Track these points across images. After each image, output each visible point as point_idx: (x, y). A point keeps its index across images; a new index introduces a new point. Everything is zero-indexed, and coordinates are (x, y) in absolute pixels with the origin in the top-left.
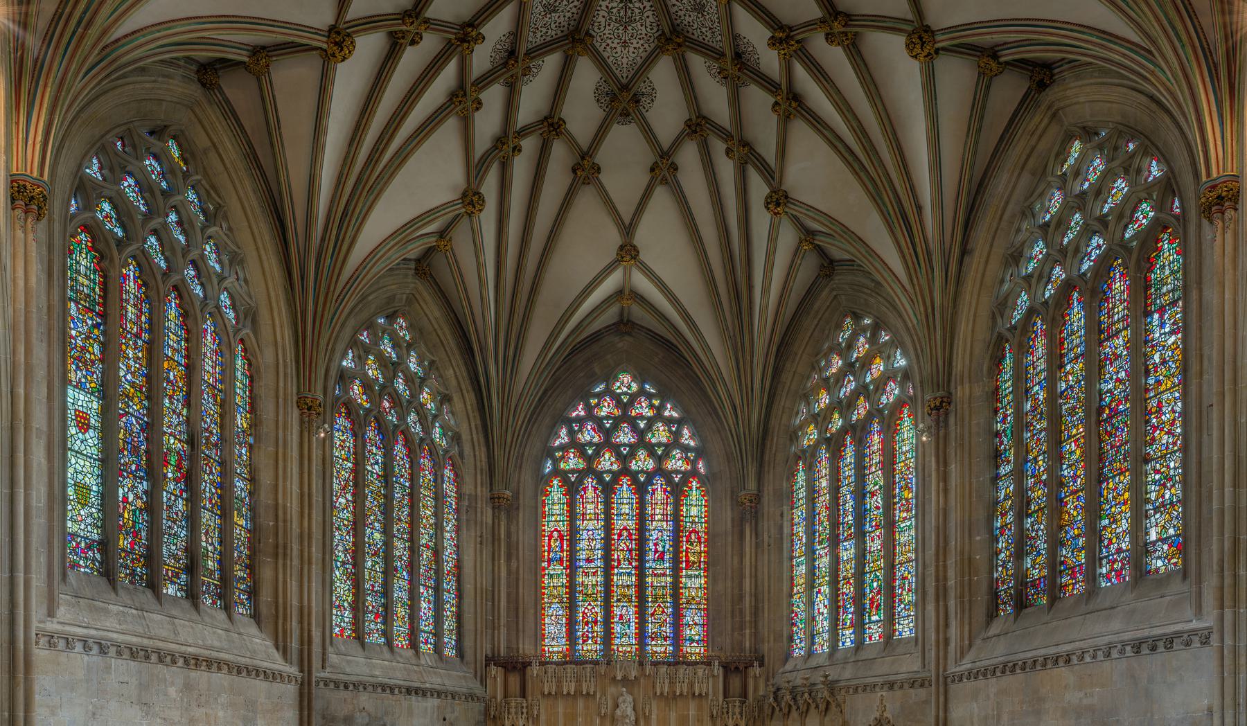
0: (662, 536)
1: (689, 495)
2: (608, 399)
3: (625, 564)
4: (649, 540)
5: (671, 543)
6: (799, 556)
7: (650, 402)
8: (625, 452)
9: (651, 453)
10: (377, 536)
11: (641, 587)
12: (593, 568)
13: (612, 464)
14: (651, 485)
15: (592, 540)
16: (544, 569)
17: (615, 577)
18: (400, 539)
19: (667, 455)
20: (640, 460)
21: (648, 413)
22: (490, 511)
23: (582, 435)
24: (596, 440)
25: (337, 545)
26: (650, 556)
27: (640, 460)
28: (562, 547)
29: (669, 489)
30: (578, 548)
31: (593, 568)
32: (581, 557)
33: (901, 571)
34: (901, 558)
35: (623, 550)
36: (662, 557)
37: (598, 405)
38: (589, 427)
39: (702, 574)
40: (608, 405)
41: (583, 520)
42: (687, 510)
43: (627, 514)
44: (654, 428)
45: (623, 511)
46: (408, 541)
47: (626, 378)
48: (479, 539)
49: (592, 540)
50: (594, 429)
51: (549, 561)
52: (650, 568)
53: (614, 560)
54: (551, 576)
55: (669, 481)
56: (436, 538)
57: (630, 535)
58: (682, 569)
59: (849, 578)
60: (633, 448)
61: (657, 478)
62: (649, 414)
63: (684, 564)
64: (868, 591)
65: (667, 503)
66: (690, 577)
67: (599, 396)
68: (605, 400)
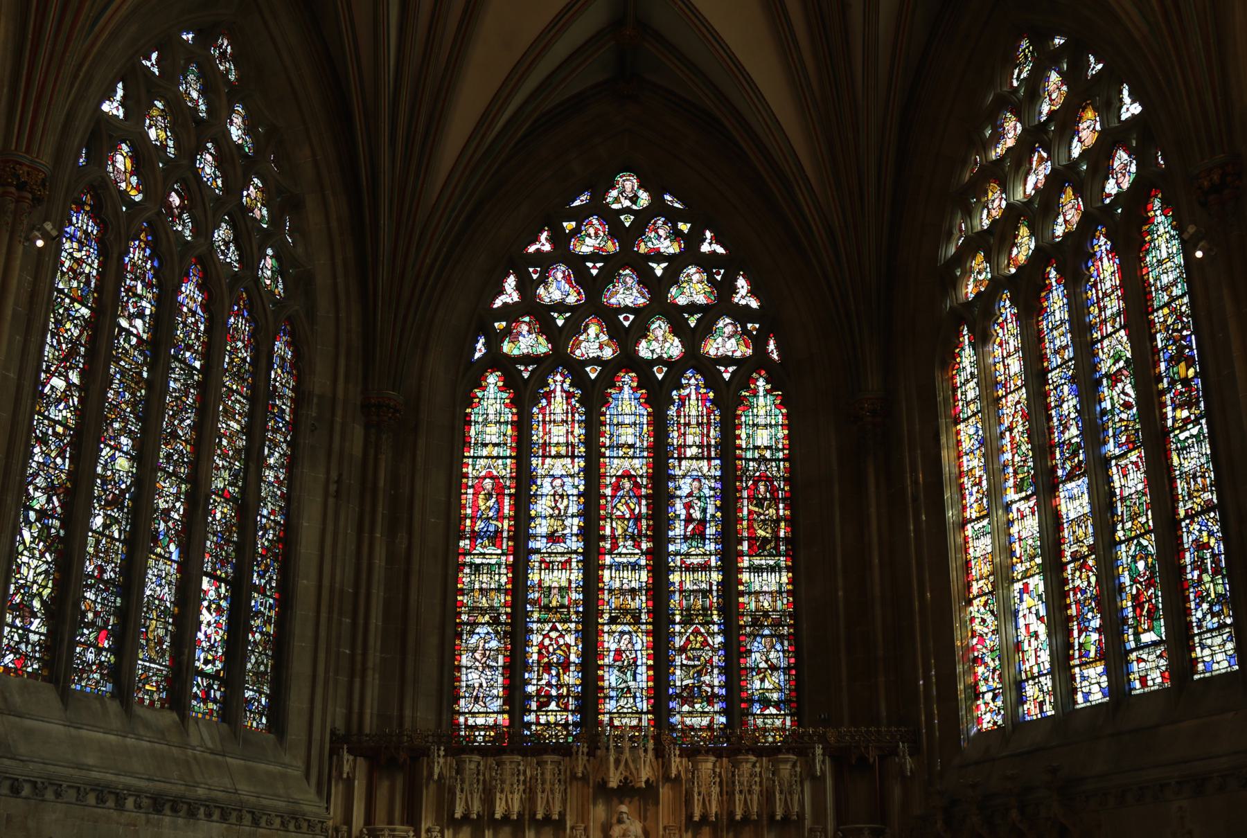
0: (700, 489)
1: (751, 407)
2: (595, 222)
3: (626, 547)
4: (674, 497)
5: (718, 503)
6: (977, 519)
7: (675, 227)
8: (626, 324)
9: (678, 328)
10: (122, 463)
11: (659, 590)
12: (562, 554)
13: (601, 348)
15: (562, 496)
17: (606, 573)
18: (170, 475)
19: (706, 329)
20: (656, 339)
21: (669, 247)
22: (358, 431)
24: (572, 299)
25: (35, 475)
26: (678, 529)
27: (656, 339)
28: (499, 510)
29: (711, 395)
30: (533, 513)
31: (562, 554)
32: (539, 530)
33: (1191, 533)
34: (1189, 505)
35: (622, 518)
36: (699, 535)
37: (576, 232)
38: (559, 275)
39: (783, 564)
40: (596, 235)
41: (544, 457)
42: (748, 436)
43: (632, 446)
44: (682, 277)
45: (622, 440)
46: (183, 481)
47: (629, 183)
48: (333, 488)
49: (562, 496)
50: (567, 279)
51: (474, 536)
52: (677, 553)
53: (604, 538)
54: (477, 568)
55: (712, 380)
56: (245, 480)
57: (637, 486)
58: (741, 554)
59: (1085, 557)
60: (643, 317)
61: (689, 374)
62: (671, 251)
63: (746, 544)
64: (1126, 580)
65: (709, 424)
66: (757, 570)
67: (581, 216)
68: (592, 225)
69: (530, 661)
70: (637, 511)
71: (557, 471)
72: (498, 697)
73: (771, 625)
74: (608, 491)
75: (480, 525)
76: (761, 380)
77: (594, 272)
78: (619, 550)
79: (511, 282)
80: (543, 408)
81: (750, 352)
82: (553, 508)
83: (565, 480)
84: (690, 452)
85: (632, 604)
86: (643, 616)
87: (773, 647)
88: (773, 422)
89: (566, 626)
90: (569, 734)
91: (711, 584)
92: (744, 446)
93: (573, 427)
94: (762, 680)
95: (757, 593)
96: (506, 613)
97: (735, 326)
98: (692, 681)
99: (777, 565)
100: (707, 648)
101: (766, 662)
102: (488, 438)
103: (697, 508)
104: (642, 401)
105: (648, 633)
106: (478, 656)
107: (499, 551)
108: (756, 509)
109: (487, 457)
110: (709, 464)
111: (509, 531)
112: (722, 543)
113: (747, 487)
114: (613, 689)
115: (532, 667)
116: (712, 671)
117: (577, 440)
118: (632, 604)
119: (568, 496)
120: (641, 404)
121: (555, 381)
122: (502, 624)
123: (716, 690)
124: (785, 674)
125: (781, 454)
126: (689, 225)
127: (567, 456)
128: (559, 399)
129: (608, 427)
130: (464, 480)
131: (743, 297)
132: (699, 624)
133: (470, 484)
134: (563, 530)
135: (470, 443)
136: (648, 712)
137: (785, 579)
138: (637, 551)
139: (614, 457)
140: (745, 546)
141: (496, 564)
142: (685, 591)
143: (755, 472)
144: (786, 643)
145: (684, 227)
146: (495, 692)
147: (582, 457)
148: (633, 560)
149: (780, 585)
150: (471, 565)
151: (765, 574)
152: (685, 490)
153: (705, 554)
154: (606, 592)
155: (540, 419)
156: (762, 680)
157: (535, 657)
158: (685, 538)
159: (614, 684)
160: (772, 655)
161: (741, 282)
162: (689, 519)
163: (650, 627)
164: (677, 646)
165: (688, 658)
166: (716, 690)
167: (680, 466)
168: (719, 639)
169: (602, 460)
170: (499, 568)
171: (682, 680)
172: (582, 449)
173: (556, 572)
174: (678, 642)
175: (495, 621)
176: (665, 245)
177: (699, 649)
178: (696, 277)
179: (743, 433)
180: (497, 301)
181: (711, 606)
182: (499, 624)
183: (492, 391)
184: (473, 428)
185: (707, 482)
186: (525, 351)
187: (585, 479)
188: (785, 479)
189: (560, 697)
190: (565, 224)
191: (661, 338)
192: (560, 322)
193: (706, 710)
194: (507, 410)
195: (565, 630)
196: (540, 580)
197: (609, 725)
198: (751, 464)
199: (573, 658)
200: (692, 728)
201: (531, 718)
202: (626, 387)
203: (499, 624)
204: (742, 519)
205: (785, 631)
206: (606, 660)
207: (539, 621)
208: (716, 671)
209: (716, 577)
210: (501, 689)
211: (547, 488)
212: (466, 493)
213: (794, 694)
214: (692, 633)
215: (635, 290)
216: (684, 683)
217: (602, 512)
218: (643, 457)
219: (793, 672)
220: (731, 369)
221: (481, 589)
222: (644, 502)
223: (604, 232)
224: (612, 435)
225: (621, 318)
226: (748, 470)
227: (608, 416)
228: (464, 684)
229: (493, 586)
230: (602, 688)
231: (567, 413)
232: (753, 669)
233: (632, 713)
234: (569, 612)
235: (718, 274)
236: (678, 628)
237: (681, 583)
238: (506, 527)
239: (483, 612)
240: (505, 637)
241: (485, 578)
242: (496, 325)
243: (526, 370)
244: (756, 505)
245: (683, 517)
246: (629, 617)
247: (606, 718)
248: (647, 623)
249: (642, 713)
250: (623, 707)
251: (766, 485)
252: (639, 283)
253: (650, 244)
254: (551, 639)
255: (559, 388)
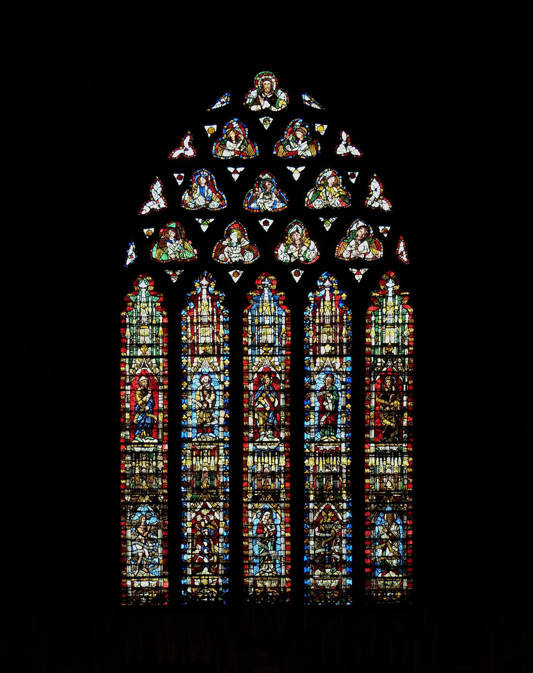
0: (332, 383)
2: (235, 125)
5: (348, 396)
7: (312, 128)
8: (266, 228)
12: (211, 443)
14: (314, 292)
15: (209, 392)
16: (128, 443)
20: (294, 244)
23: (191, 195)
24: (215, 205)
26: (313, 420)
27: (294, 244)
28: (154, 404)
29: (344, 296)
30: (184, 406)
31: (211, 443)
32: (190, 422)
35: (263, 410)
37: (217, 135)
38: (203, 181)
39: (405, 450)
40: (237, 139)
41: (193, 356)
42: (377, 334)
43: (272, 345)
45: (263, 339)
49: (209, 392)
52: (312, 441)
53: (247, 428)
54: (137, 456)
57: (276, 381)
58: (369, 441)
61: (324, 276)
62: (309, 154)
63: (373, 432)
69: (186, 534)
70: (276, 404)
71: (206, 369)
72: (159, 564)
73: (393, 503)
74: (251, 386)
75: (138, 418)
76: (391, 281)
77: (236, 177)
78: (261, 438)
79: (157, 188)
80: (191, 310)
81: (380, 254)
82: (202, 402)
83: (212, 376)
84: (324, 350)
85: (273, 485)
86: (282, 496)
87: (394, 521)
88: (400, 321)
89: (215, 504)
90: (219, 593)
91: (341, 468)
92: (373, 344)
93: (218, 328)
94: (384, 549)
95: (381, 476)
96: (163, 494)
97: (367, 228)
98: (324, 550)
99: (400, 450)
100: (337, 522)
101: (388, 534)
102: (142, 338)
103: (330, 401)
104: (281, 302)
105: (285, 510)
106: (140, 530)
107: (156, 441)
108: (383, 401)
109: (141, 357)
110: (341, 361)
111: (163, 423)
112: (351, 431)
113: (375, 382)
114: (256, 557)
115: (187, 539)
116: (341, 542)
117: (222, 340)
118: (273, 485)
119: (215, 391)
120: (279, 306)
121: (201, 285)
122: (160, 503)
123: (344, 557)
124: (403, 544)
125: (406, 350)
126: (326, 127)
127: (213, 355)
128: (205, 302)
129: (250, 328)
130: (123, 378)
131: (376, 200)
132: (330, 502)
133: (128, 381)
134: (211, 421)
135: (126, 344)
136: (286, 576)
137: (406, 463)
138: (276, 439)
139: (255, 356)
140: (372, 434)
141: (154, 451)
142: (318, 474)
143: (382, 367)
144: (405, 518)
145: (321, 129)
146: (156, 560)
147: (227, 355)
148: (272, 447)
149: (402, 468)
150: (132, 453)
151: (388, 459)
152: (320, 385)
153: (336, 442)
154: (249, 475)
155: (189, 321)
156: (384, 549)
157: (189, 530)
158: (319, 428)
159: (257, 553)
160: (393, 528)
161: (375, 185)
162: (323, 411)
163: (287, 505)
164: (311, 521)
165: (320, 531)
166: (344, 557)
167: (315, 363)
168: (348, 515)
169: (244, 358)
170: (156, 456)
171: (315, 550)
172: (227, 348)
173: (205, 459)
174: (312, 518)
175: (154, 501)
176: (303, 148)
177: (330, 523)
178: (331, 181)
179: (372, 332)
180: (145, 208)
181: (341, 487)
182: (158, 503)
183: (144, 295)
184: (128, 329)
185: (339, 377)
186: (173, 256)
187: (230, 376)
188: (409, 374)
189: (210, 564)
190: (207, 128)
191: (298, 242)
192: (204, 228)
193: (335, 574)
194: (158, 313)
195: (215, 508)
196: (192, 465)
197: (252, 586)
198: (379, 360)
199: (221, 531)
200: (323, 589)
201: (188, 581)
202: (266, 290)
203: (158, 503)
204: (370, 410)
205: (405, 507)
206: (250, 533)
207: (192, 500)
208: (344, 542)
209: (345, 461)
210: (161, 558)
211: (196, 384)
212: (125, 390)
213: (410, 561)
214: (323, 510)
215: (274, 195)
216: (317, 552)
217: (245, 405)
218: (282, 355)
219: (411, 542)
220: (362, 271)
221: (141, 474)
222: (282, 396)
223: (244, 135)
224: (253, 335)
225: (261, 222)
226: (376, 366)
227: (250, 318)
228: (130, 554)
229: (151, 471)
230: (247, 556)
231: (213, 315)
232: (376, 540)
233: (272, 576)
234: (217, 492)
235: (353, 176)
236: (311, 506)
237: (315, 466)
238: (161, 419)
239: (143, 493)
240: (163, 514)
241: (144, 464)
242: (145, 231)
243: (174, 274)
244: (382, 398)
245: (317, 409)
246: (269, 496)
247: (250, 581)
248: (285, 502)
249: (281, 576)
250: (265, 572)
251: (392, 380)
252: (277, 187)
253: (288, 147)
254: (203, 516)
255: (204, 292)
